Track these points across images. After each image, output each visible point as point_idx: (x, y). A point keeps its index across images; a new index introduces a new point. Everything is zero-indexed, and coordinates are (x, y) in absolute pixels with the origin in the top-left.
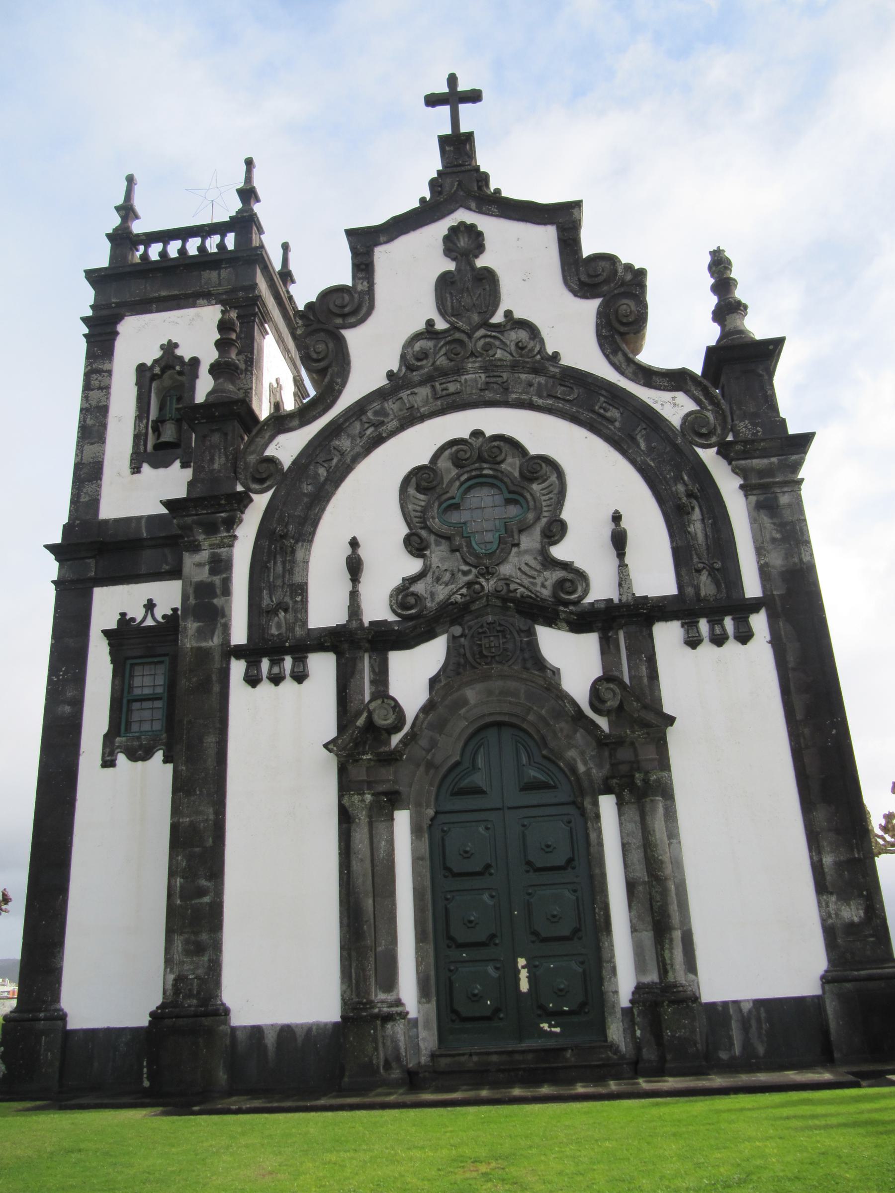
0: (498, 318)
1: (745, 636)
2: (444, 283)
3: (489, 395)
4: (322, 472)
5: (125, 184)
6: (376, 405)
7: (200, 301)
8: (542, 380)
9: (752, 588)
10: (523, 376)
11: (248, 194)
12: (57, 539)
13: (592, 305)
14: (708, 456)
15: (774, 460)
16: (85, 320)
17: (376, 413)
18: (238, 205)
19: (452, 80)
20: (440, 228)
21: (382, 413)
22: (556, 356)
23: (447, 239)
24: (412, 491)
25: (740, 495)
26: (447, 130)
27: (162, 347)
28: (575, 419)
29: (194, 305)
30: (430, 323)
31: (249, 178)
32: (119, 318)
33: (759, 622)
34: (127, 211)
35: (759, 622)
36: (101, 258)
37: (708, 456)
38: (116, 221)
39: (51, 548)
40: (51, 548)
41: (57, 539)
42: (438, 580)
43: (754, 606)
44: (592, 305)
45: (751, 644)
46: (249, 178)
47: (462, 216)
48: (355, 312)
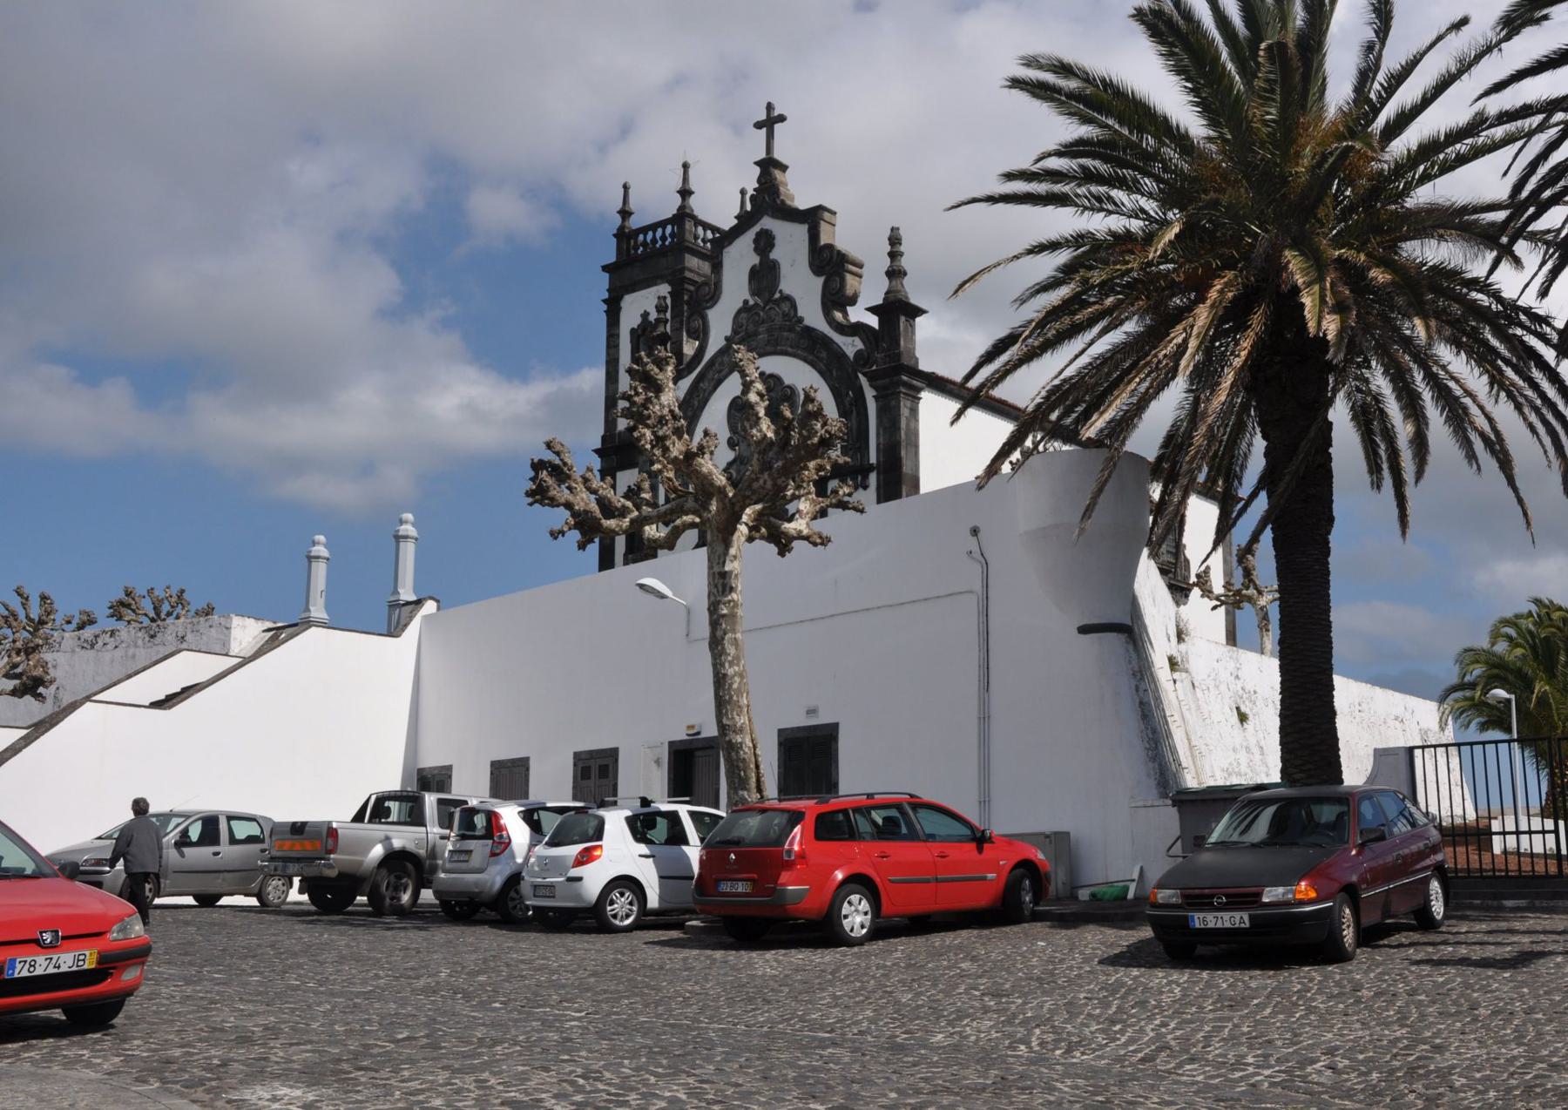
0: (777, 295)
1: (865, 487)
2: (754, 273)
3: (769, 348)
4: (696, 403)
5: (622, 190)
6: (719, 359)
7: (659, 281)
8: (792, 335)
9: (873, 459)
10: (785, 334)
11: (685, 193)
12: (599, 445)
13: (820, 281)
14: (863, 380)
15: (887, 380)
16: (604, 301)
17: (720, 365)
18: (678, 200)
19: (770, 107)
20: (750, 235)
21: (722, 364)
22: (801, 320)
23: (756, 241)
24: (733, 411)
25: (873, 400)
26: (762, 155)
27: (642, 315)
28: (805, 360)
29: (656, 284)
30: (746, 302)
31: (685, 179)
32: (620, 298)
33: (873, 477)
34: (625, 213)
35: (873, 477)
36: (611, 257)
37: (863, 380)
38: (618, 220)
39: (596, 451)
40: (596, 451)
41: (599, 445)
42: (742, 463)
43: (871, 468)
44: (820, 281)
45: (868, 490)
46: (685, 179)
47: (767, 223)
48: (711, 298)
